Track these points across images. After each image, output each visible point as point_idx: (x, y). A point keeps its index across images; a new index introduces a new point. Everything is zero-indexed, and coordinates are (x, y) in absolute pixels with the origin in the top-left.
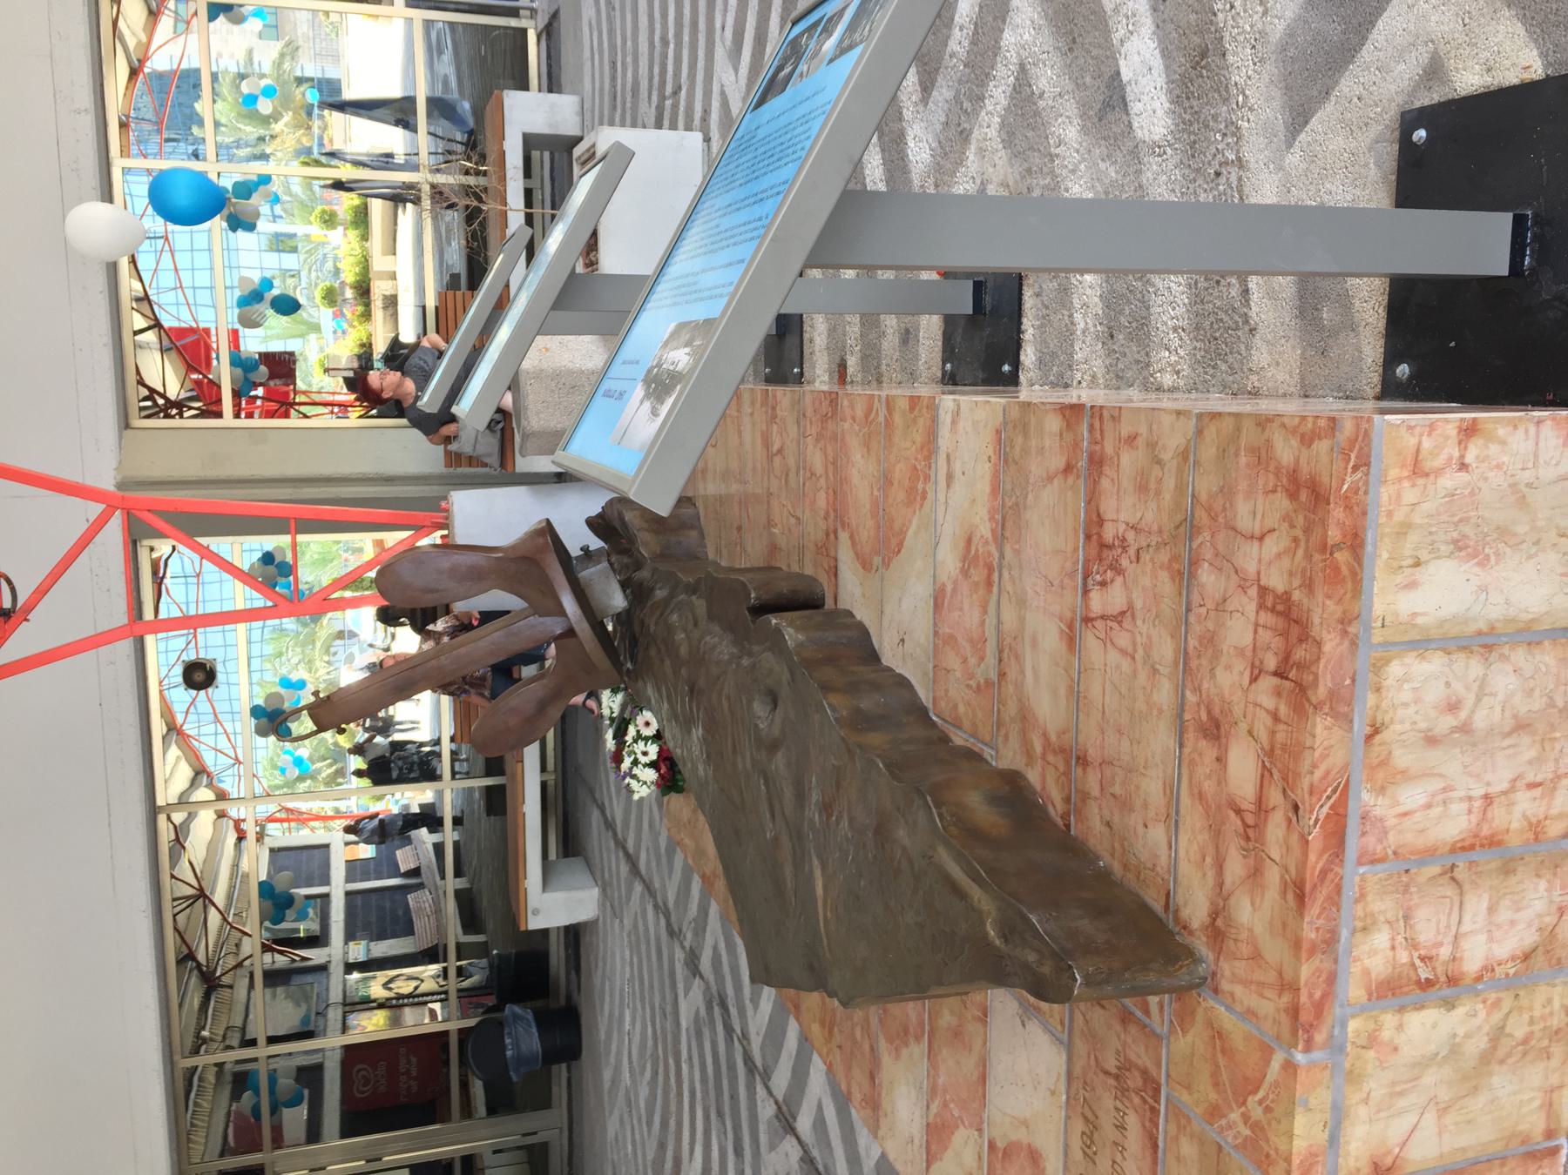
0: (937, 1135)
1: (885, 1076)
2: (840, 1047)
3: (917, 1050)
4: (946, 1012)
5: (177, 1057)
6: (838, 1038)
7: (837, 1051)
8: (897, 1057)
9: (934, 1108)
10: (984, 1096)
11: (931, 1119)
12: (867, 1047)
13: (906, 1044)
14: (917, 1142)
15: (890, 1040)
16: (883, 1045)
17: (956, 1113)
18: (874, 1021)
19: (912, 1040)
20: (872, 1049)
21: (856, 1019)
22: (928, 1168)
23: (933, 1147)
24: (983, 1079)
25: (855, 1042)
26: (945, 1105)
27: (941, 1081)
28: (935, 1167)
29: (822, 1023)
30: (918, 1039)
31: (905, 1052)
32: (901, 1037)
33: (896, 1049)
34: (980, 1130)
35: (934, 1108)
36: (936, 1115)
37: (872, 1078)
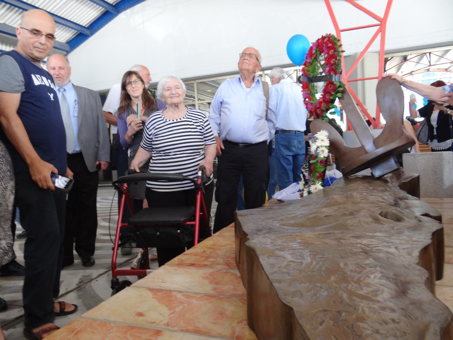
0: (165, 295)
1: (193, 270)
2: (204, 251)
3: (208, 288)
4: (233, 308)
5: (197, 81)
6: (208, 251)
7: (202, 250)
8: (204, 278)
9: (179, 296)
10: (187, 331)
11: (174, 293)
12: (206, 263)
13: (211, 283)
14: (163, 285)
15: (211, 274)
16: (208, 271)
17: (177, 310)
18: (219, 267)
19: (213, 286)
20: (205, 265)
21: (218, 259)
22: (151, 290)
23: (160, 294)
24: (197, 332)
25: (208, 258)
26: (181, 303)
27: (194, 301)
28: (150, 294)
29: (214, 245)
30: (214, 289)
31: (206, 282)
32: (215, 281)
33: (207, 277)
34: (168, 325)
35: (179, 296)
36: (175, 296)
37: (192, 265)
